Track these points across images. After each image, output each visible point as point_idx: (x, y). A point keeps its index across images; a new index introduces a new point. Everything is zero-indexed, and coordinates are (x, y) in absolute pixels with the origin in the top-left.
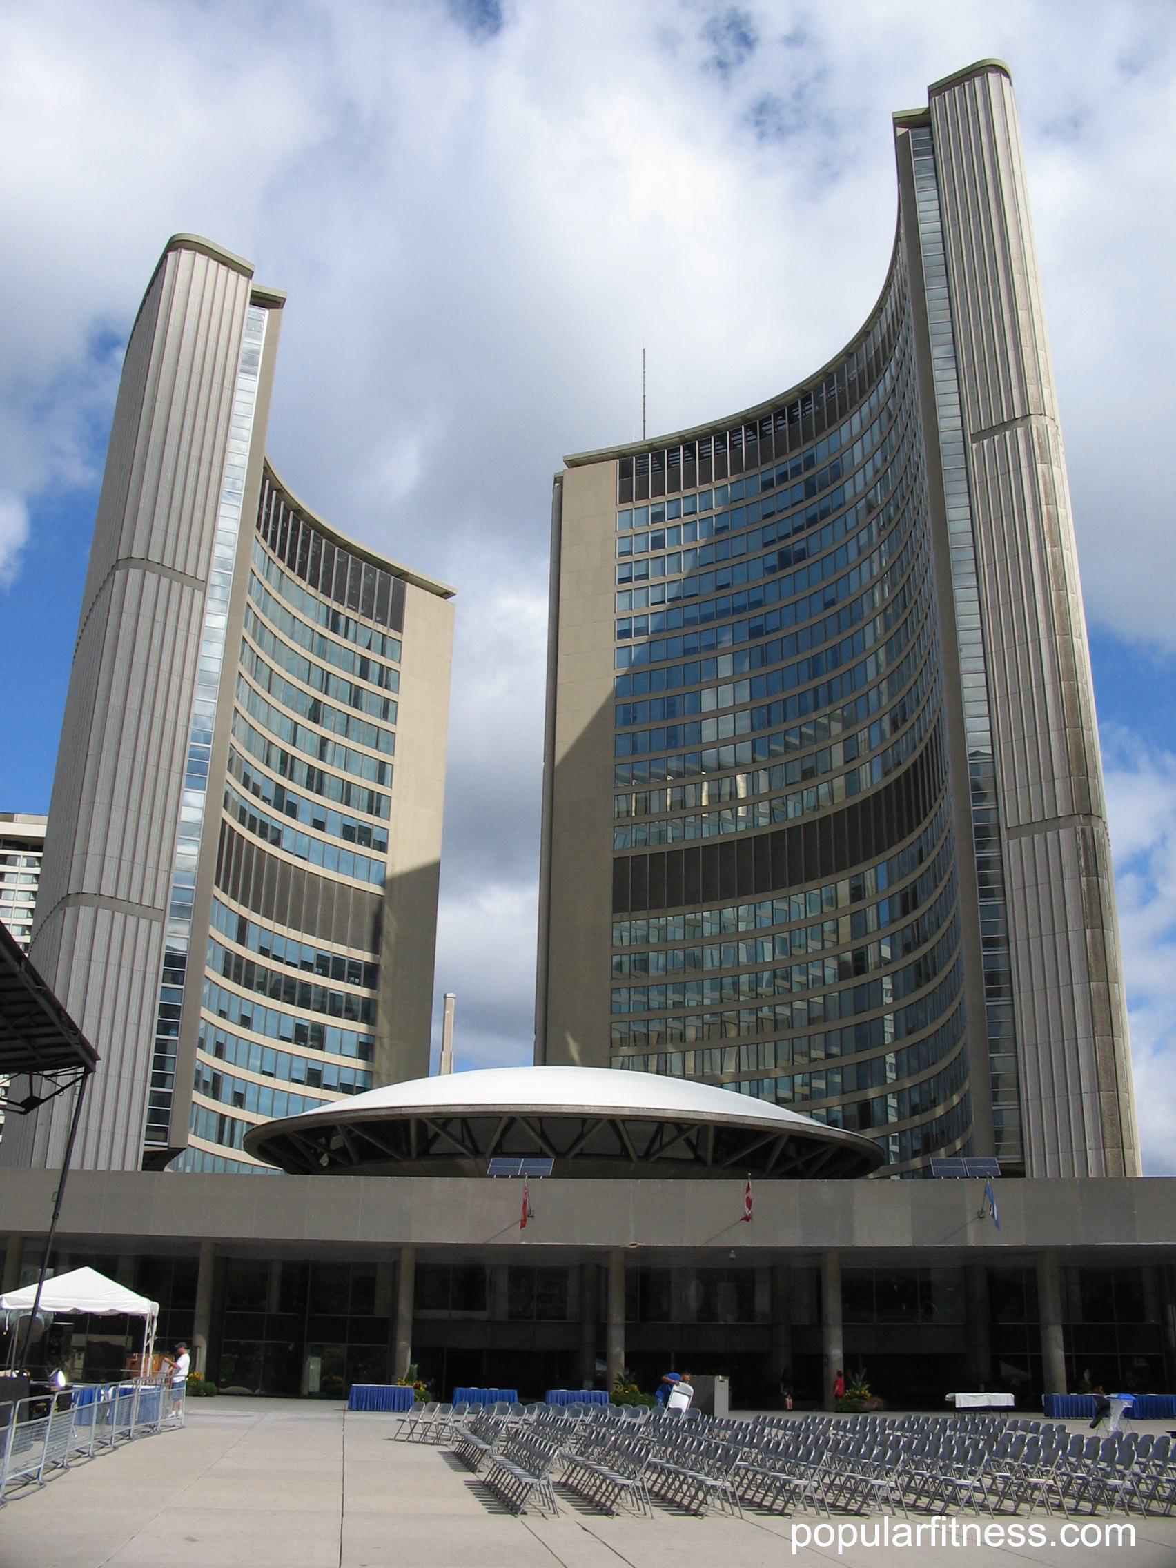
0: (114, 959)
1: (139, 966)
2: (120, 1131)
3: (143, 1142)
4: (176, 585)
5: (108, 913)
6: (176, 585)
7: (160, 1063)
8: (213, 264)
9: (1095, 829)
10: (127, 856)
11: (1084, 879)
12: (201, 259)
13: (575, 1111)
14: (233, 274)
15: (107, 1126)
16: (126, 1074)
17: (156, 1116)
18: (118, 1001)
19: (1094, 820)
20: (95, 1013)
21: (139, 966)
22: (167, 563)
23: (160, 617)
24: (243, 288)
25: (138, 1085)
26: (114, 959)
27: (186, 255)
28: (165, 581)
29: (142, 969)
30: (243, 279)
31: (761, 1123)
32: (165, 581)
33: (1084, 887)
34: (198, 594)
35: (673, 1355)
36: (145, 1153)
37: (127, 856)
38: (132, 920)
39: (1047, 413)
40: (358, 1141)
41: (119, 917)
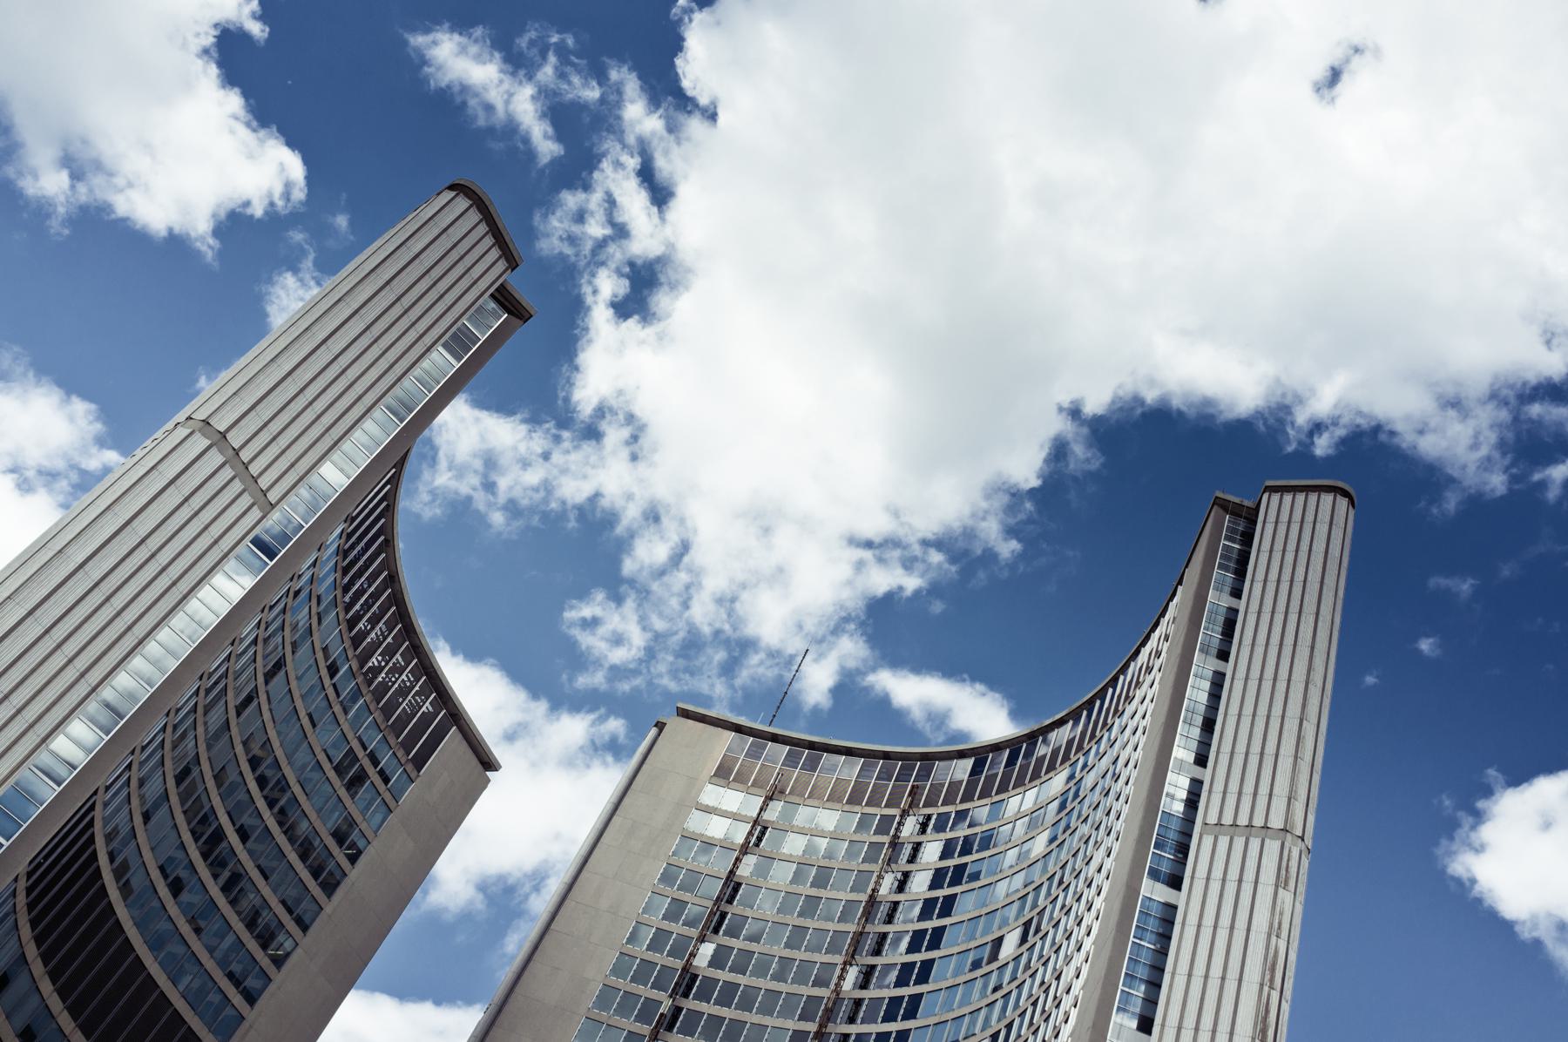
4: (237, 486)
6: (237, 486)
8: (483, 228)
12: (474, 216)
14: (495, 253)
22: (245, 455)
27: (462, 203)
28: (227, 473)
30: (502, 265)
32: (227, 473)
34: (256, 513)
39: (1305, 838)
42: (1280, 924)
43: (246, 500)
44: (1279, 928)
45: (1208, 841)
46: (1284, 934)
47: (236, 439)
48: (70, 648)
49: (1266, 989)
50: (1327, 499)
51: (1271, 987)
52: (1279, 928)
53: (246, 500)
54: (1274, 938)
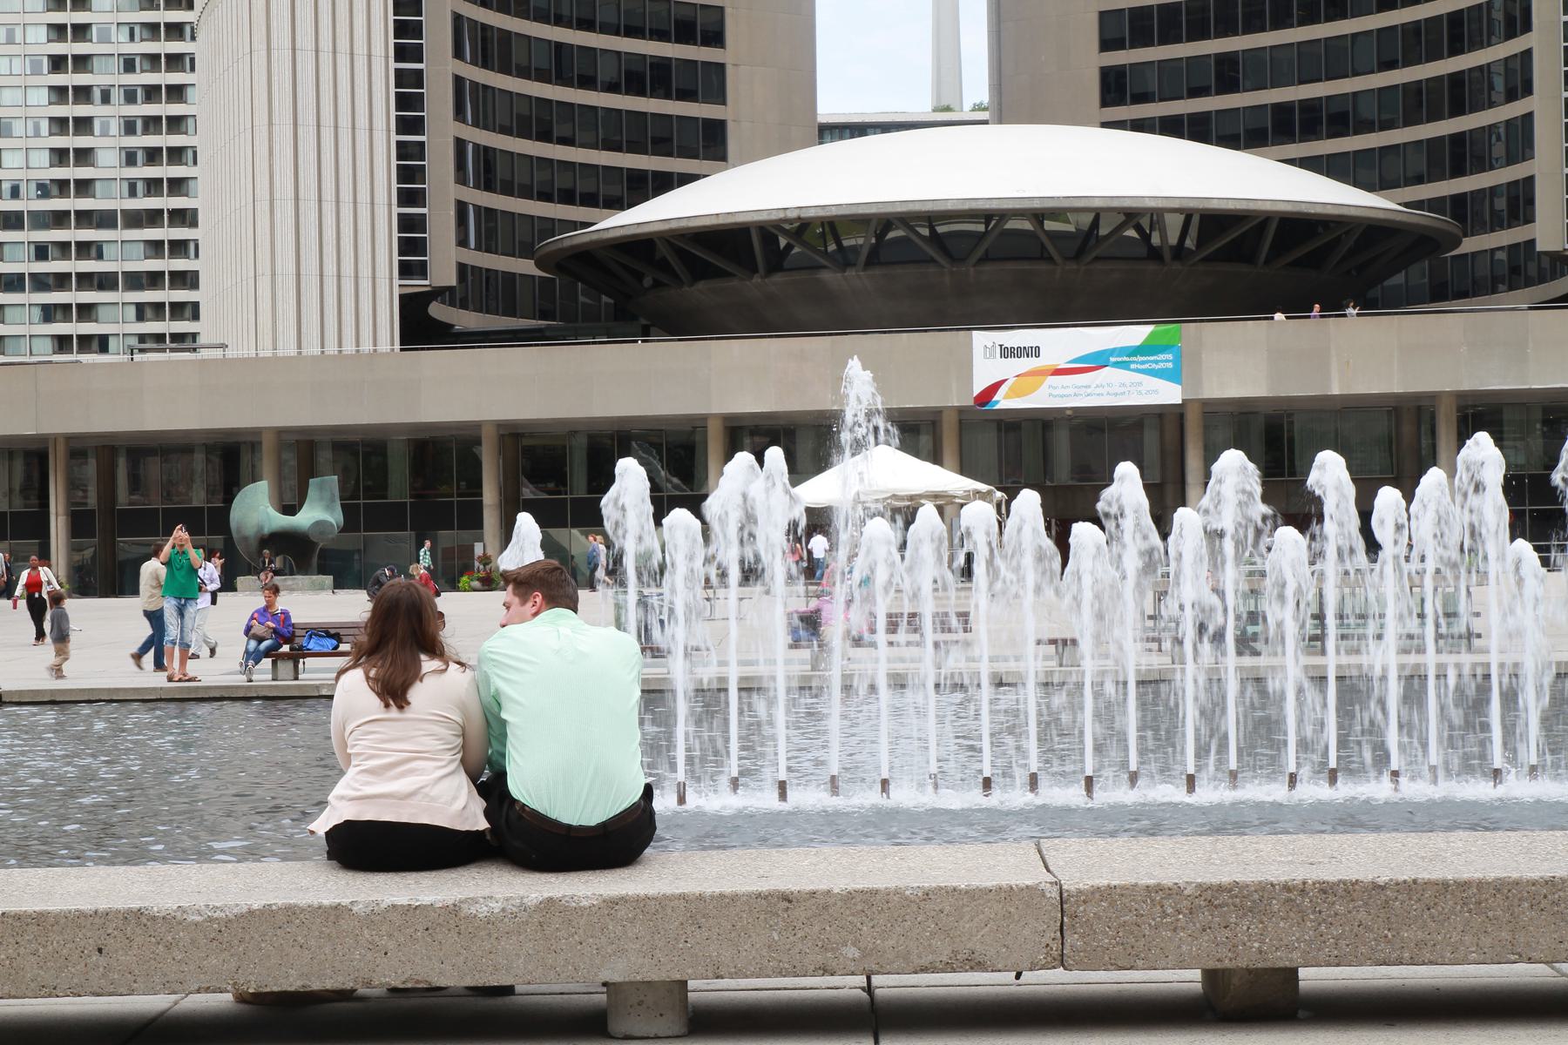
0: (325, 44)
1: (360, 48)
2: (365, 272)
3: (397, 282)
7: (406, 174)
13: (966, 206)
15: (348, 268)
16: (364, 196)
17: (407, 247)
18: (340, 101)
20: (312, 120)
21: (360, 48)
25: (381, 212)
26: (325, 44)
29: (365, 52)
31: (1231, 206)
35: (1053, 521)
36: (401, 297)
40: (681, 254)
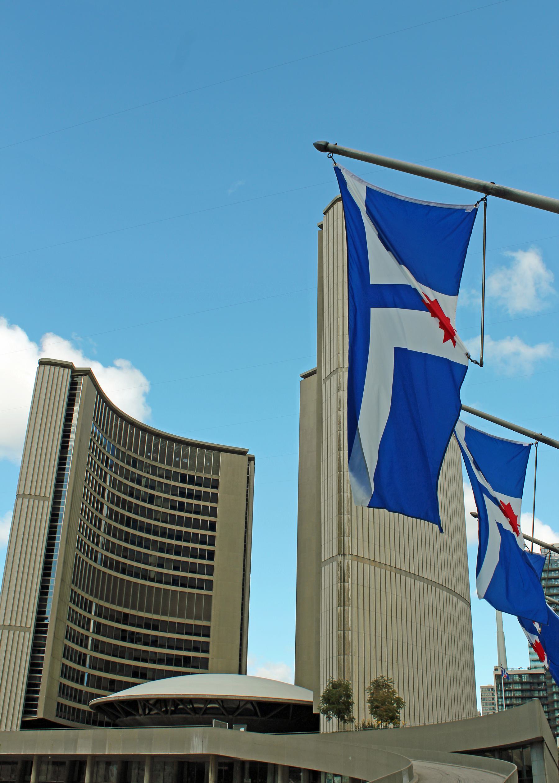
4: (36, 501)
5: (7, 631)
8: (53, 367)
9: (346, 561)
10: (15, 609)
11: (339, 584)
12: (48, 367)
19: (347, 557)
23: (29, 515)
24: (67, 372)
27: (42, 367)
30: (66, 370)
33: (339, 588)
34: (46, 503)
37: (15, 609)
38: (17, 633)
41: (12, 632)
42: (340, 405)
43: (41, 502)
44: (340, 407)
45: (324, 385)
46: (342, 409)
47: (27, 492)
48: (26, 571)
49: (339, 432)
50: (335, 206)
51: (340, 430)
52: (340, 407)
53: (41, 502)
54: (339, 412)
